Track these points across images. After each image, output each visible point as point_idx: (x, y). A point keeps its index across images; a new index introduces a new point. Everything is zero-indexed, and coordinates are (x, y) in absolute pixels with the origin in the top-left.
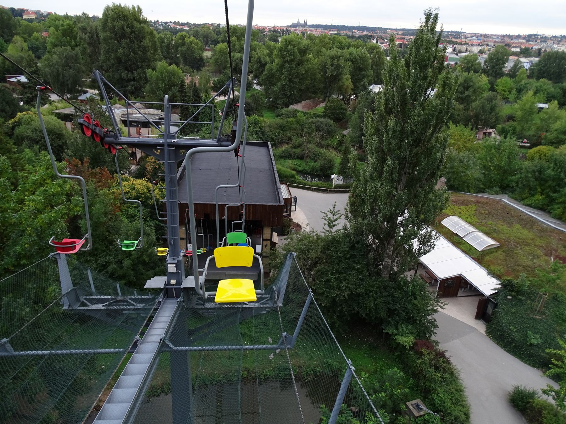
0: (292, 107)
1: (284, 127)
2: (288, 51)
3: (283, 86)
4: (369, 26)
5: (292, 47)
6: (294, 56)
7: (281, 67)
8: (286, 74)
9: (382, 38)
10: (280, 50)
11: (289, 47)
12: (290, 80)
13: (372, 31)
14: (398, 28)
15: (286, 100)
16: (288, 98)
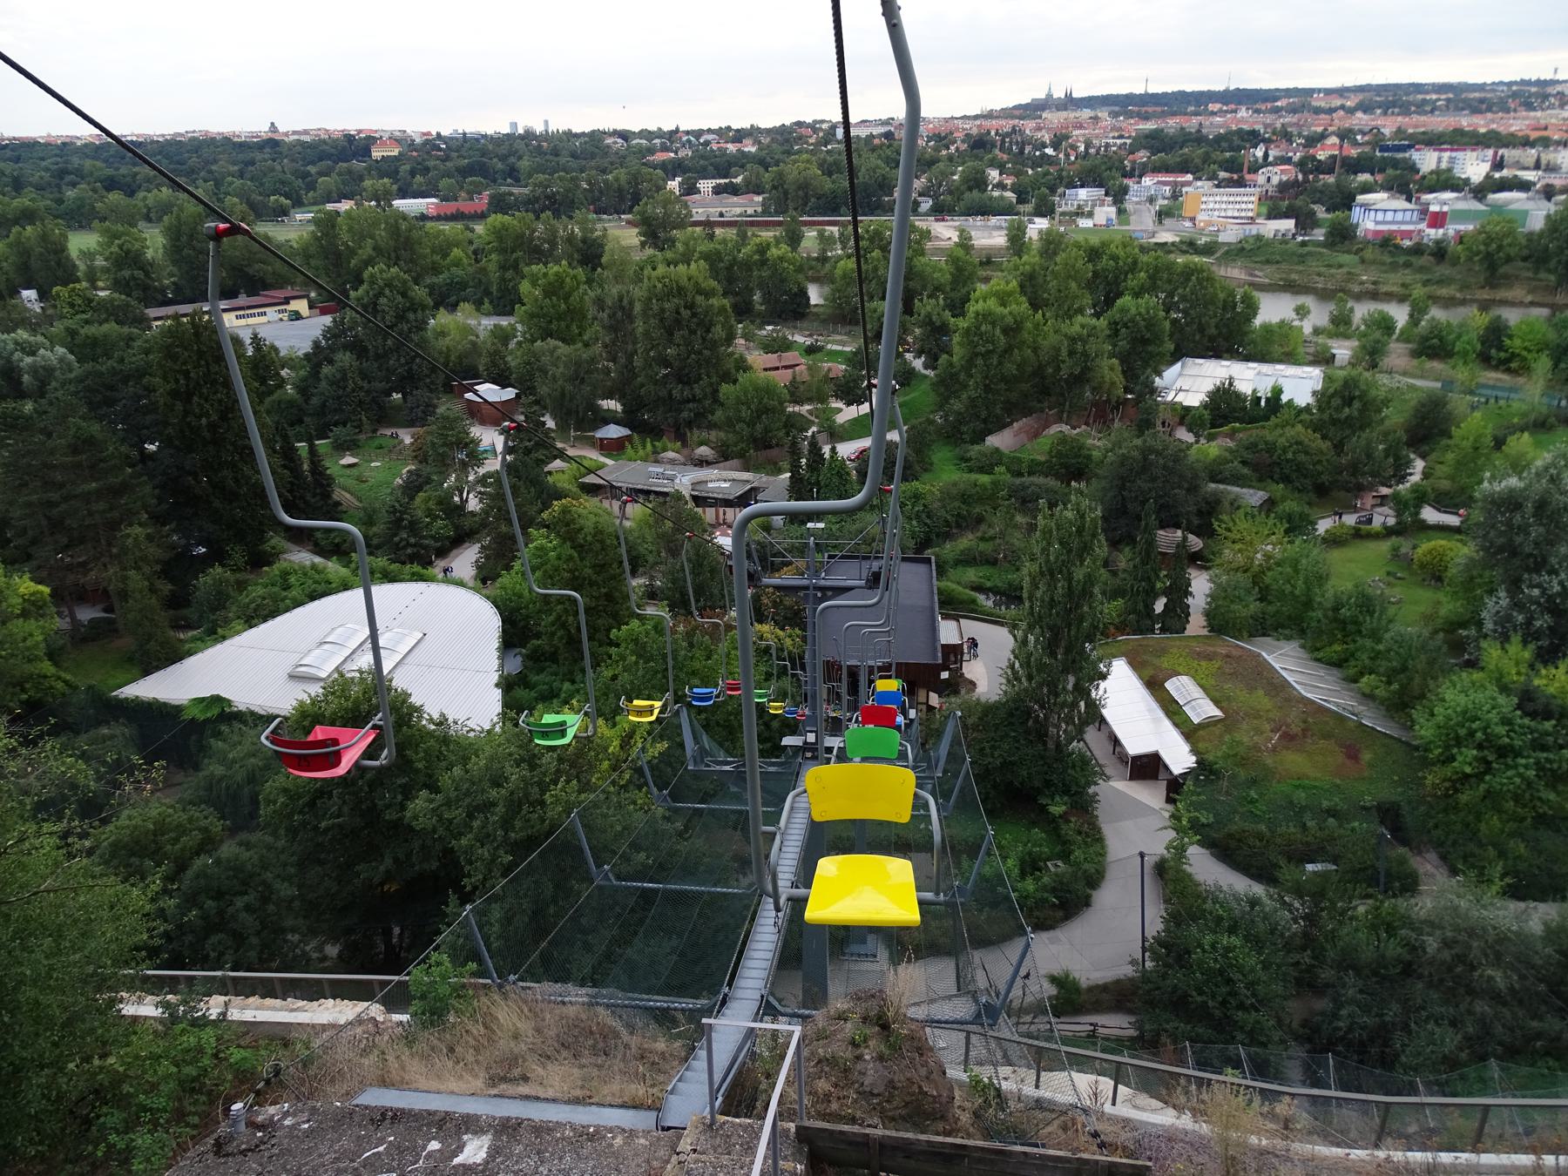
0: (993, 441)
1: (969, 496)
2: (981, 335)
3: (972, 400)
4: (1257, 87)
5: (989, 327)
6: (993, 344)
7: (970, 362)
8: (979, 378)
9: (1286, 136)
10: (967, 331)
11: (983, 328)
12: (987, 388)
13: (1266, 100)
14: (1349, 83)
15: (981, 426)
16: (985, 421)
